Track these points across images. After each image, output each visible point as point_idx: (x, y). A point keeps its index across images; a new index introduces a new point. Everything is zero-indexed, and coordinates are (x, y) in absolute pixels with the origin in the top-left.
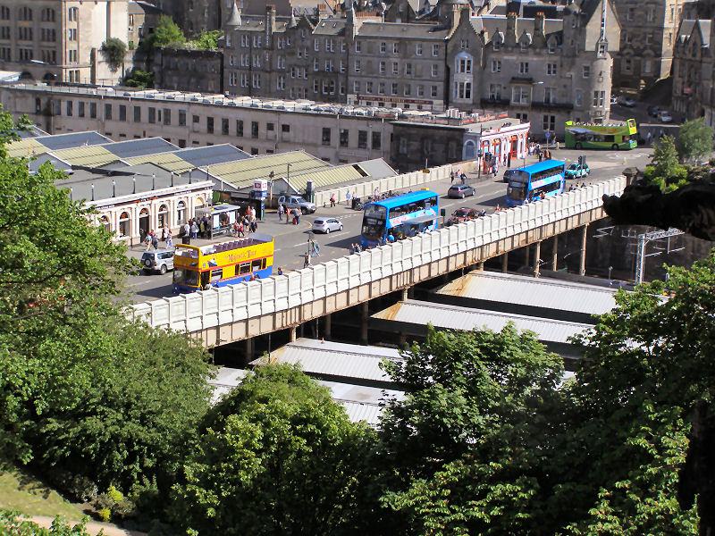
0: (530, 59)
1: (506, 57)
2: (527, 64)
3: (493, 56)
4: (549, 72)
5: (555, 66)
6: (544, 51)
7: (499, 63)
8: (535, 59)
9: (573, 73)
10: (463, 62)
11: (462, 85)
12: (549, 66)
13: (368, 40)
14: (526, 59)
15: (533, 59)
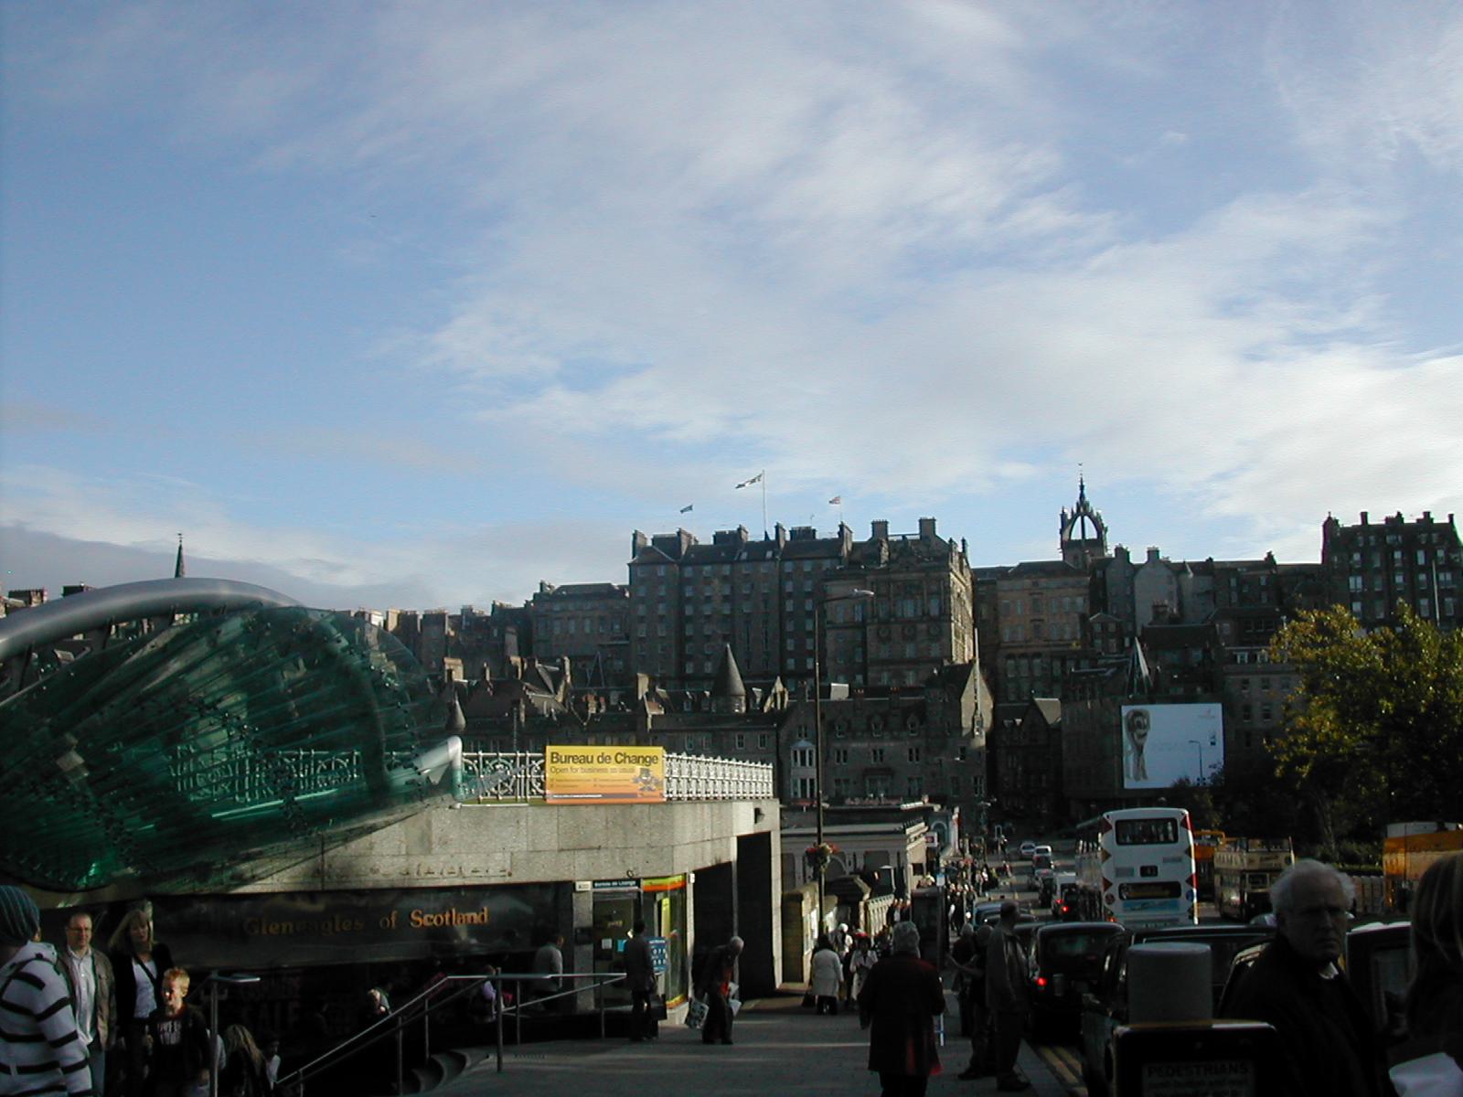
0: (886, 744)
1: (854, 745)
2: (881, 752)
3: (838, 745)
4: (911, 759)
5: (917, 751)
6: (904, 734)
7: (845, 753)
8: (892, 744)
9: (943, 758)
10: (803, 753)
11: (804, 782)
12: (911, 752)
13: (668, 734)
14: (878, 745)
15: (889, 745)
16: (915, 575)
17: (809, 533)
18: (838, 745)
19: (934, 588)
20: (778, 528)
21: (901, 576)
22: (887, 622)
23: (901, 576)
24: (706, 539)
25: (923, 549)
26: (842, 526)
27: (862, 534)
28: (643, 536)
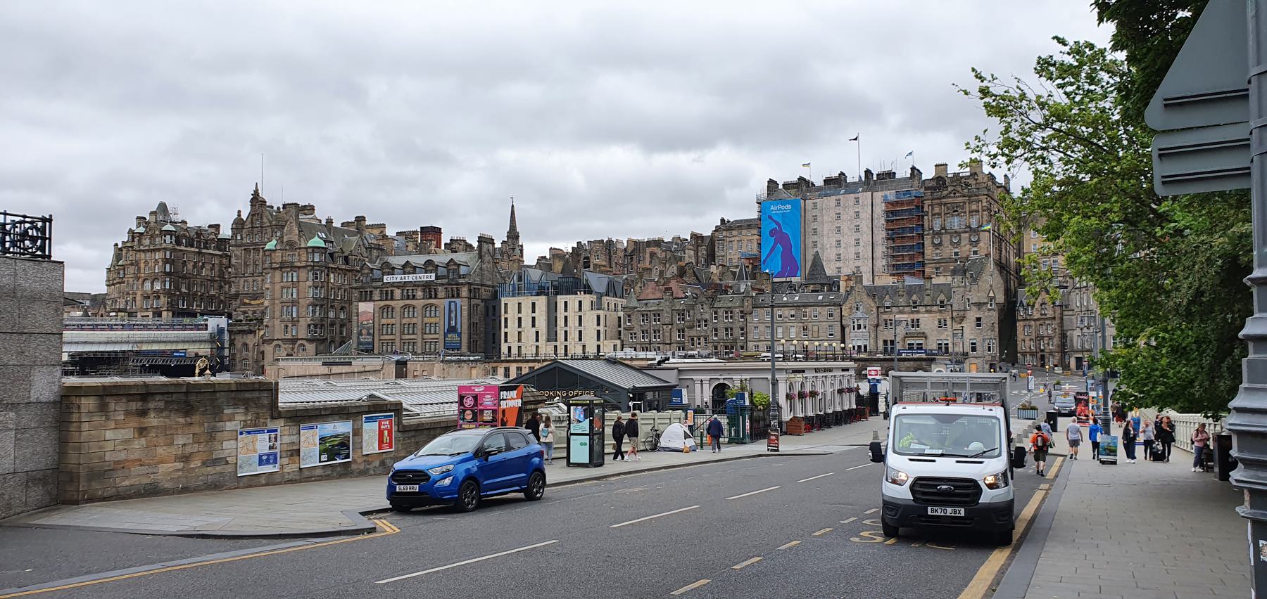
6: (935, 308)
14: (916, 316)
16: (960, 199)
17: (891, 175)
18: (885, 317)
19: (974, 207)
20: (868, 172)
21: (950, 200)
22: (939, 233)
23: (950, 200)
24: (819, 182)
25: (972, 181)
26: (913, 169)
27: (928, 173)
28: (776, 182)
